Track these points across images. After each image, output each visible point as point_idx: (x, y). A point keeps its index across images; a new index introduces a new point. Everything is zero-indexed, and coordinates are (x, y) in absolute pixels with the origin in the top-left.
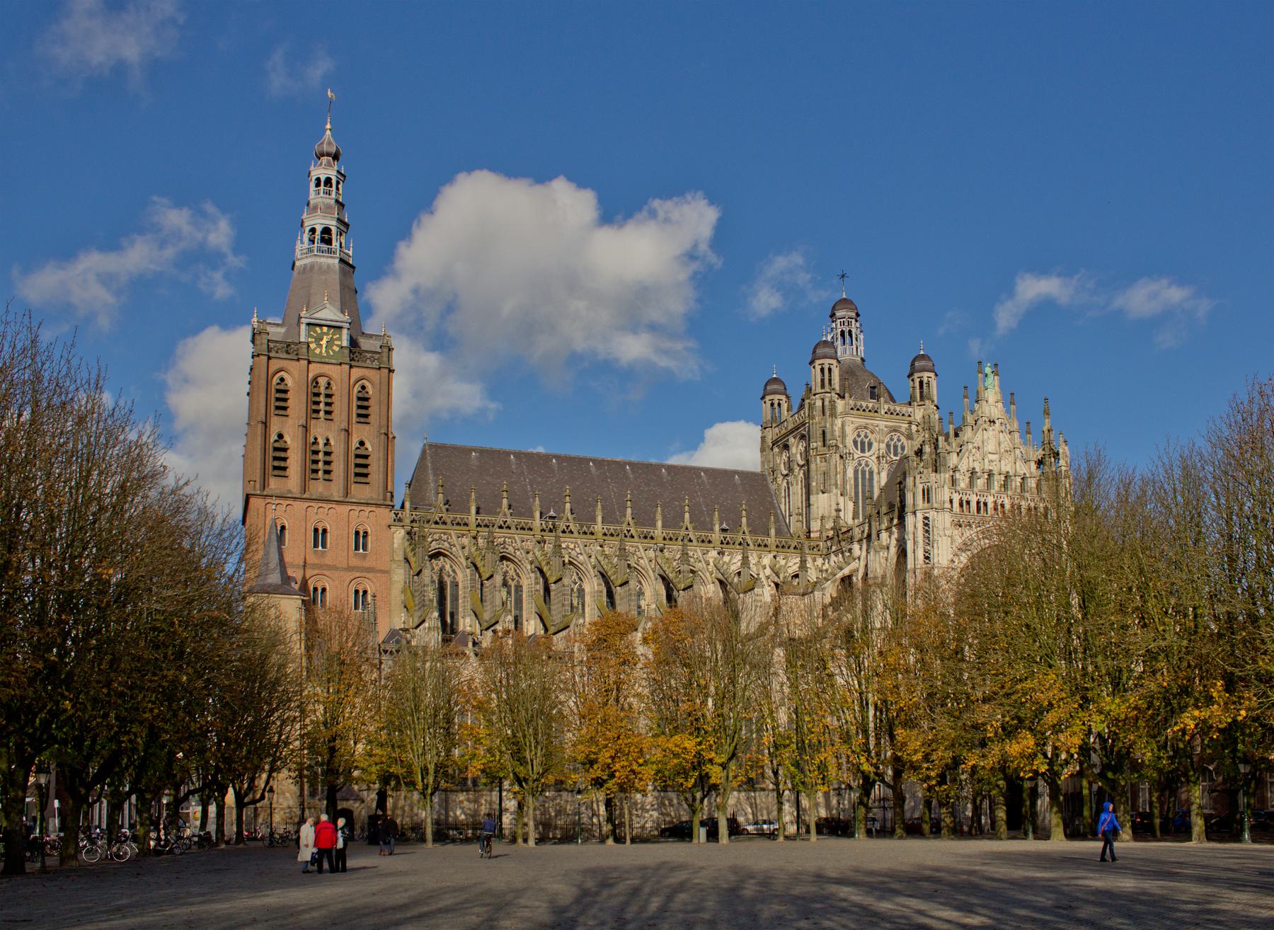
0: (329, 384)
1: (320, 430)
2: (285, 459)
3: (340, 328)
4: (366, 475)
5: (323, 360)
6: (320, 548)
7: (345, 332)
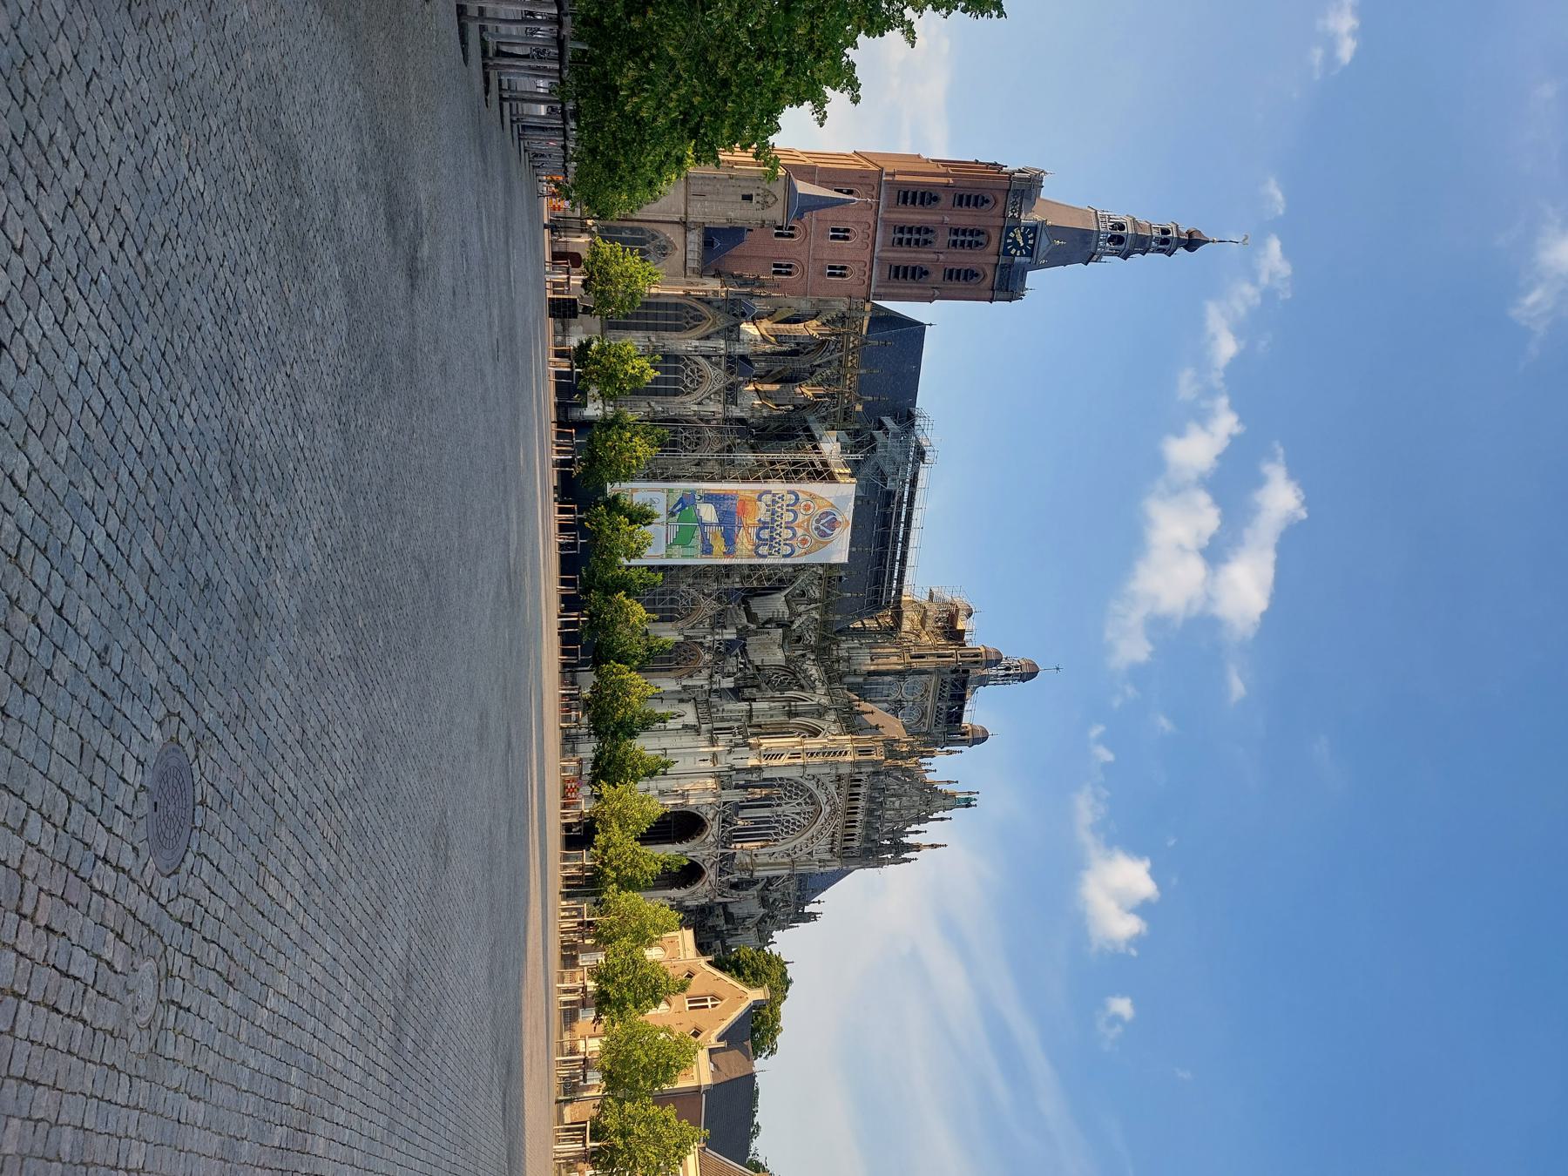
0: (981, 244)
1: (942, 239)
2: (913, 202)
3: (1032, 256)
4: (896, 276)
5: (1003, 240)
6: (831, 234)
7: (1028, 260)
